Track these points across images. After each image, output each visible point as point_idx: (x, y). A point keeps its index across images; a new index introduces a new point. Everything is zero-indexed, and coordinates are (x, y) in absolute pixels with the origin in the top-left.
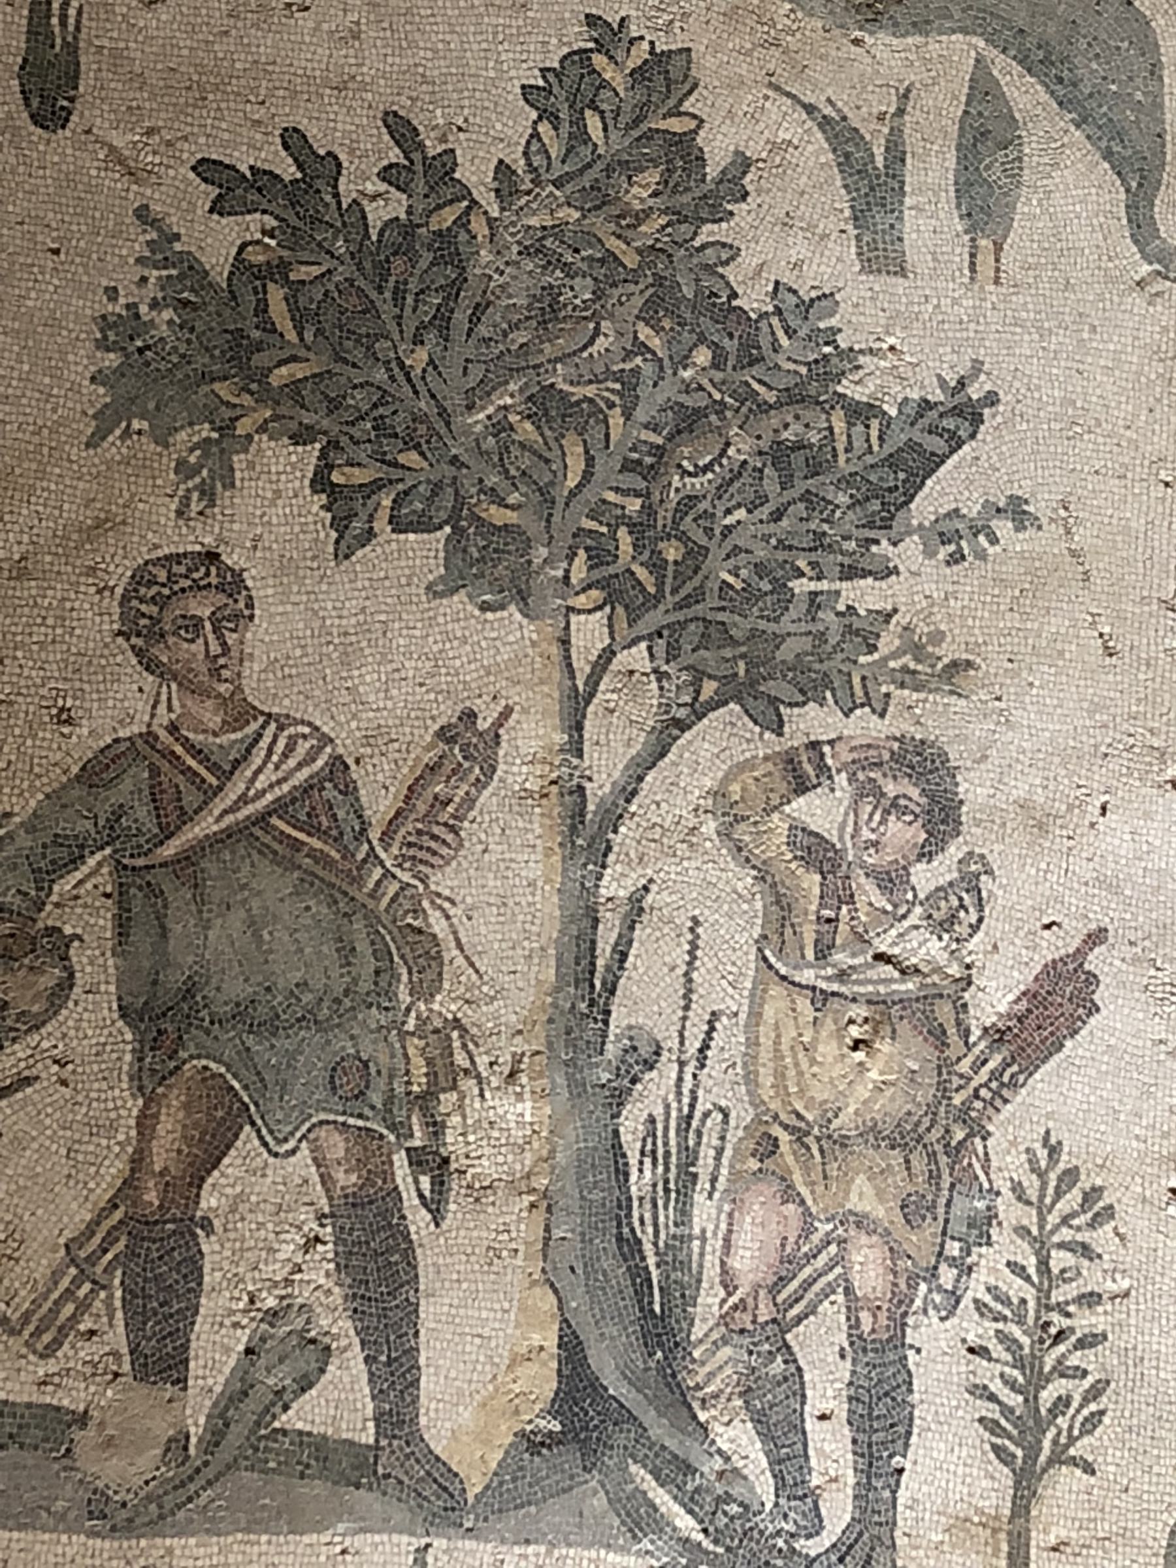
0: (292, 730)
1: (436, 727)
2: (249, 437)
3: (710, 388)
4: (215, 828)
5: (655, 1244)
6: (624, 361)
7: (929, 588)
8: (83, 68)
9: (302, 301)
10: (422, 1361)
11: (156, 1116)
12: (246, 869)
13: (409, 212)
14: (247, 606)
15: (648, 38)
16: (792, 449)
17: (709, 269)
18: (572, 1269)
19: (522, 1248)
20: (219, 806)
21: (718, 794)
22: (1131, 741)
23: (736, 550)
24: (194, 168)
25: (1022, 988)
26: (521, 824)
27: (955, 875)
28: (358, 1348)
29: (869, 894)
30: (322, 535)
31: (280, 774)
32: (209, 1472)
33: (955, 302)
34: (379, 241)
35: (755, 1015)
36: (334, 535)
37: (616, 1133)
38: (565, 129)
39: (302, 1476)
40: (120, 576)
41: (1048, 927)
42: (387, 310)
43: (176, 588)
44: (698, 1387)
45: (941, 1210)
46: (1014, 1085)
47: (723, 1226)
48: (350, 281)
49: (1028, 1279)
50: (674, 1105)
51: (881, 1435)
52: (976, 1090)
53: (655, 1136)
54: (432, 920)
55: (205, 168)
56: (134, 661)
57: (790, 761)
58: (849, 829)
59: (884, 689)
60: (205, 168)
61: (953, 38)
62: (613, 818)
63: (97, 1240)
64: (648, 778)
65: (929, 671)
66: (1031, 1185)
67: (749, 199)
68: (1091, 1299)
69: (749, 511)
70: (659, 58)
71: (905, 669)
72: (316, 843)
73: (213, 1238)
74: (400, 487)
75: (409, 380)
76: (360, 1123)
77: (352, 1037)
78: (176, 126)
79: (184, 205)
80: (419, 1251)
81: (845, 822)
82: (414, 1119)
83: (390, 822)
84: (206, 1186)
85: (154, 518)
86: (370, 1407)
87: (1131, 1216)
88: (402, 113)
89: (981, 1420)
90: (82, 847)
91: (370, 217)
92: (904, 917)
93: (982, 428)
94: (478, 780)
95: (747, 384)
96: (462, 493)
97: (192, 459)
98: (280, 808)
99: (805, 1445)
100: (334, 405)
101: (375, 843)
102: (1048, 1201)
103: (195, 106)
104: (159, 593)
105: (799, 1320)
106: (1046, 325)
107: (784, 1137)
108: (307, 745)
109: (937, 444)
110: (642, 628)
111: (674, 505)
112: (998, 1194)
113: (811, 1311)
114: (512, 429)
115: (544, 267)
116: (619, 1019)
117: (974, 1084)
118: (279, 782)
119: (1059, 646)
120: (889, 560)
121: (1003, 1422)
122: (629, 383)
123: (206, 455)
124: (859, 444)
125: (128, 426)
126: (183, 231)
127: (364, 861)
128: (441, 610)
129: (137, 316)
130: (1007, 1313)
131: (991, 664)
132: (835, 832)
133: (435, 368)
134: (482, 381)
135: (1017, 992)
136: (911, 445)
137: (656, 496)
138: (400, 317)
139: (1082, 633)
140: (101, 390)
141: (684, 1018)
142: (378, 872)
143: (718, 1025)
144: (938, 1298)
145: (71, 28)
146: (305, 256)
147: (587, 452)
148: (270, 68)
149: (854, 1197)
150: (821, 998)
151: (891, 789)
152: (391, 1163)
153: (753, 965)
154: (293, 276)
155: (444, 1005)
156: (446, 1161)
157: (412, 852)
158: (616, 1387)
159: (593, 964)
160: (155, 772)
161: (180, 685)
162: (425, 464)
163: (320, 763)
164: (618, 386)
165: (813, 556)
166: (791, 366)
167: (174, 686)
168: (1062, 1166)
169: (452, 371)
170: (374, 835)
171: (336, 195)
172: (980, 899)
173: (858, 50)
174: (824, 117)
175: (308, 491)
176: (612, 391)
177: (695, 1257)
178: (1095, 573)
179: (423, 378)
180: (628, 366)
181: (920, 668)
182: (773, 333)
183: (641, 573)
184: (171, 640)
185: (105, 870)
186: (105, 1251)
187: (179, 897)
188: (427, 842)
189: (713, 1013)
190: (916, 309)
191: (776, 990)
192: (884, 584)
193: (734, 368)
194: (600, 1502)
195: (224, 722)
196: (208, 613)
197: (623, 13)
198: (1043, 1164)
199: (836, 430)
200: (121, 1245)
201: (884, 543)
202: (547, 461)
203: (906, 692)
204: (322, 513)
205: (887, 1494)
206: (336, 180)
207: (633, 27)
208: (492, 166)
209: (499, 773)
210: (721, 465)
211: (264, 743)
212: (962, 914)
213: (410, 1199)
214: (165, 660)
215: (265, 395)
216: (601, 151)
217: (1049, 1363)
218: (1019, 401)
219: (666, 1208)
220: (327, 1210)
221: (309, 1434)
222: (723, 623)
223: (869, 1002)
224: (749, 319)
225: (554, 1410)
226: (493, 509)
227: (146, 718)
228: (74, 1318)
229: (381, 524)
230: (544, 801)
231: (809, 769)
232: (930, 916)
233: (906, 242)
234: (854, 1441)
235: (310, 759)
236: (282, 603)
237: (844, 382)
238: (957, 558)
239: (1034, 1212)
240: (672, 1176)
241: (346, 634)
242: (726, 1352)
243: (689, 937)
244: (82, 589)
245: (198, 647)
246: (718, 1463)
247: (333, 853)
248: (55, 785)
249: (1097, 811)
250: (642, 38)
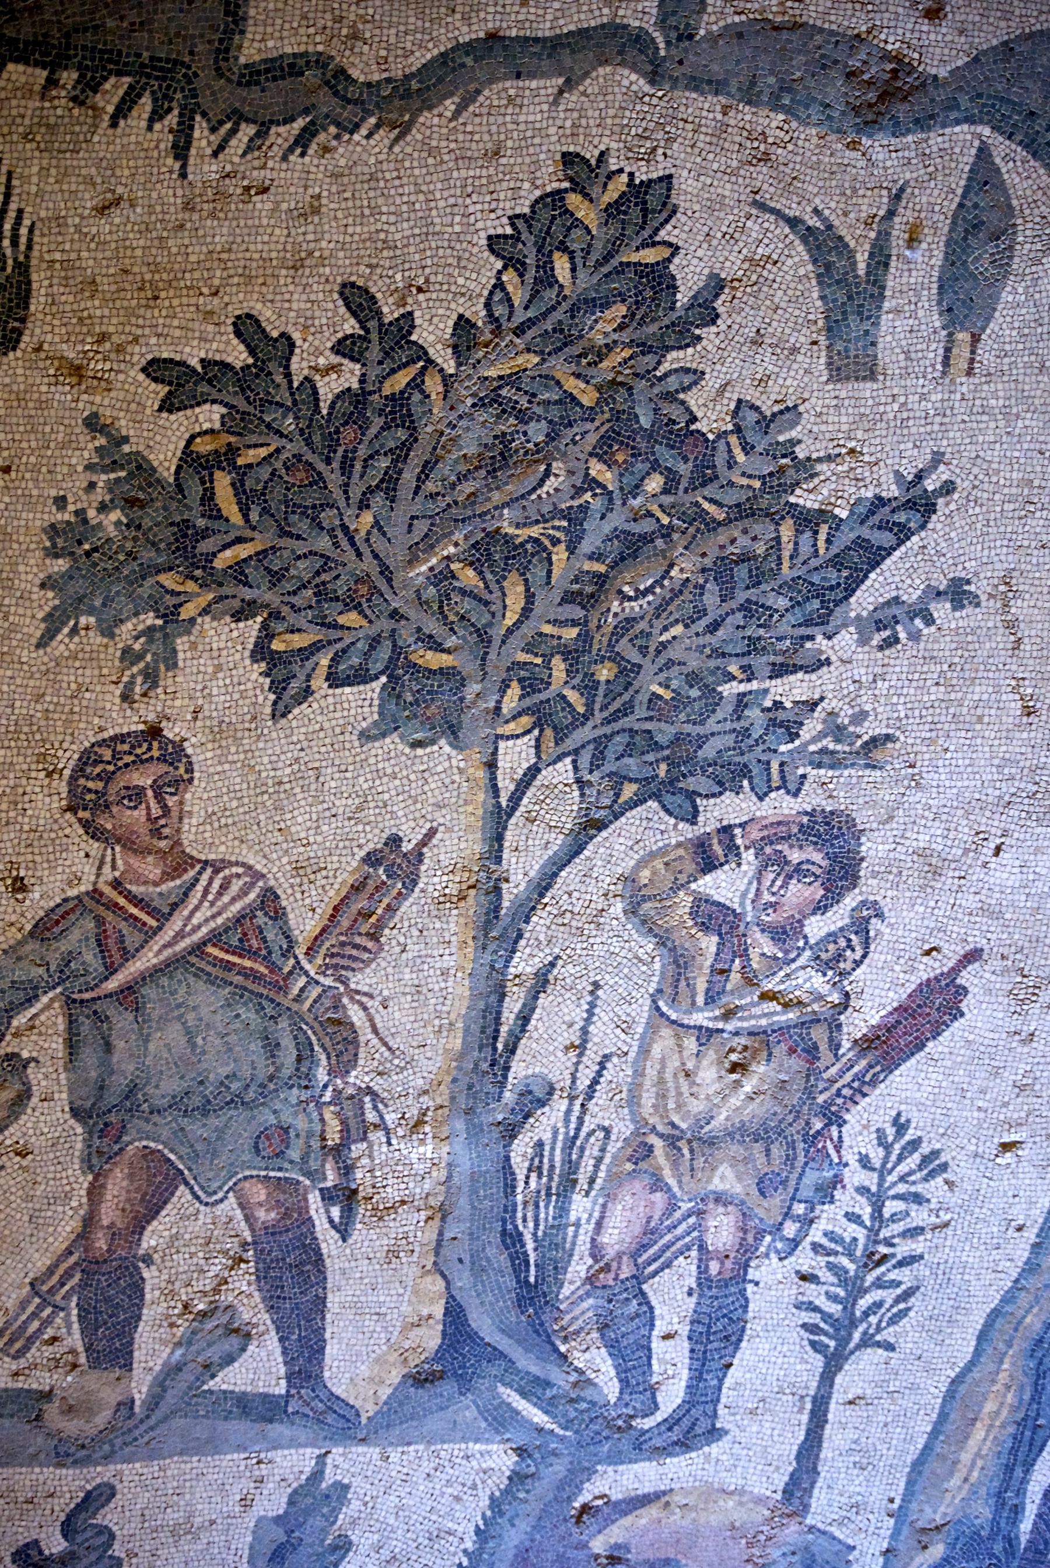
0: (227, 872)
1: (363, 853)
2: (192, 621)
3: (659, 514)
4: (155, 961)
5: (535, 1235)
6: (572, 498)
8: (35, 286)
9: (249, 484)
10: (327, 1335)
11: (103, 1186)
12: (182, 990)
13: (362, 381)
14: (187, 771)
15: (627, 169)
16: (736, 563)
17: (670, 397)
18: (460, 1261)
19: (417, 1249)
21: (629, 880)
22: (1035, 788)
23: (670, 664)
24: (143, 370)
25: (895, 1004)
26: (438, 925)
27: (847, 921)
28: (273, 1333)
29: (762, 945)
30: (261, 699)
31: (215, 910)
32: (152, 1421)
33: (923, 397)
34: (329, 414)
36: (272, 697)
37: (507, 1158)
38: (531, 274)
39: (226, 1418)
41: (928, 953)
42: (334, 478)
43: (120, 764)
44: (563, 1328)
45: (792, 1183)
46: (874, 1083)
47: (596, 1215)
48: (298, 457)
49: (861, 1224)
50: (562, 1130)
51: (716, 1345)
52: (839, 1090)
53: (542, 1156)
54: (351, 1013)
55: (155, 369)
56: (81, 831)
58: (751, 896)
59: (801, 771)
60: (155, 369)
61: (957, 129)
62: (527, 910)
63: (55, 1279)
64: (563, 874)
65: (847, 749)
66: (877, 1156)
67: (719, 322)
69: (687, 626)
70: (638, 190)
71: (823, 751)
72: (248, 963)
73: (153, 1268)
74: (339, 646)
75: (353, 544)
76: (280, 1174)
77: (275, 1112)
78: (127, 329)
79: (133, 406)
80: (328, 1262)
81: (747, 891)
82: (328, 1166)
83: (316, 938)
84: (147, 1233)
85: (100, 704)
86: (282, 1370)
88: (360, 283)
89: (804, 1326)
90: (36, 988)
91: (321, 391)
92: (793, 960)
93: (934, 517)
94: (400, 894)
95: (697, 504)
96: (400, 643)
97: (137, 646)
98: (215, 938)
99: (649, 1358)
100: (276, 577)
101: (301, 957)
102: (889, 1166)
103: (147, 307)
104: (104, 771)
105: (656, 1273)
106: (1014, 410)
107: (658, 1143)
108: (241, 883)
110: (569, 744)
111: (610, 629)
112: (846, 1165)
113: (668, 1265)
114: (454, 577)
115: (498, 416)
116: (519, 1070)
117: (838, 1085)
118: (213, 917)
119: (979, 712)
120: (821, 652)
121: (822, 1325)
122: (576, 518)
123: (151, 640)
124: (805, 549)
125: (76, 624)
126: (132, 433)
127: (291, 973)
128: (373, 752)
129: (85, 521)
130: (840, 1249)
132: (736, 900)
133: (380, 529)
134: (426, 535)
135: (889, 1009)
136: (860, 543)
137: (593, 624)
138: (347, 485)
139: (1004, 697)
140: (50, 594)
141: (578, 1063)
142: (302, 981)
143: (609, 1065)
144: (779, 1245)
145: (22, 248)
146: (253, 439)
147: (527, 590)
148: (225, 256)
149: (716, 1180)
150: (706, 1035)
152: (306, 1200)
153: (646, 1015)
154: (240, 462)
155: (357, 1077)
156: (355, 1192)
157: (334, 961)
159: (497, 1031)
160: (100, 921)
161: (124, 846)
162: (365, 623)
163: (252, 896)
164: (565, 524)
165: (745, 661)
166: (745, 481)
167: (118, 849)
168: (907, 1138)
169: (396, 530)
170: (300, 951)
171: (288, 375)
172: (868, 938)
173: (854, 154)
174: (809, 228)
175: (248, 662)
176: (558, 528)
177: (569, 1239)
178: (1026, 640)
179: (367, 540)
180: (576, 503)
181: (839, 747)
182: (730, 451)
183: (572, 696)
184: (115, 809)
185: (56, 1005)
186: (63, 1285)
187: (122, 1020)
188: (349, 951)
189: (605, 1056)
190: (882, 409)
191: (666, 1032)
192: (814, 677)
193: (686, 491)
194: (471, 1413)
195: (164, 873)
196: (149, 782)
197: (602, 147)
198: (890, 1139)
199: (785, 539)
200: (76, 1279)
201: (819, 638)
202: (487, 603)
203: (822, 772)
204: (261, 680)
205: (715, 1382)
206: (289, 360)
207: (612, 161)
208: (451, 323)
209: (421, 885)
210: (662, 586)
211: (199, 888)
212: (848, 953)
213: (321, 1224)
214: (109, 826)
215: (210, 579)
216: (567, 292)
217: (870, 1279)
218: (974, 487)
219: (547, 1207)
220: (249, 1239)
221: (232, 1392)
222: (649, 732)
223: (750, 1034)
224: (707, 440)
225: (439, 1355)
226: (430, 654)
227: (93, 878)
228: (40, 1331)
229: (318, 682)
230: (462, 904)
231: (718, 849)
232: (818, 957)
233: (880, 346)
234: (692, 1351)
235: (244, 892)
236: (220, 763)
237: (798, 492)
238: (892, 642)
239: (876, 1175)
240: (554, 1185)
241: (280, 783)
242: (591, 1301)
243: (589, 998)
244: (33, 774)
245: (140, 814)
246: (573, 1377)
247: (263, 970)
248: (12, 942)
249: (991, 853)
250: (621, 171)
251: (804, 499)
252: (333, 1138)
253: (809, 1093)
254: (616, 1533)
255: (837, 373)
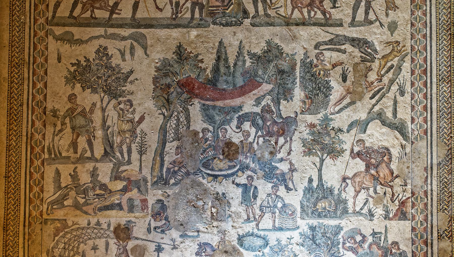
7: (130, 87)
20: (76, 112)
21: (113, 106)
29: (126, 112)
35: (118, 123)
40: (67, 96)
46: (139, 125)
57: (119, 102)
62: (105, 109)
68: (146, 141)
70: (105, 47)
87: (148, 135)
98: (80, 112)
109: (130, 75)
116: (107, 124)
122: (104, 74)
131: (135, 92)
136: (127, 75)
150: (123, 121)
151: (127, 103)
155: (94, 125)
158: (108, 151)
187: (73, 119)
213: (92, 139)
238: (132, 84)
251: (122, 72)
252: (92, 131)
253: (133, 127)
254: (124, 174)
255: (123, 61)
